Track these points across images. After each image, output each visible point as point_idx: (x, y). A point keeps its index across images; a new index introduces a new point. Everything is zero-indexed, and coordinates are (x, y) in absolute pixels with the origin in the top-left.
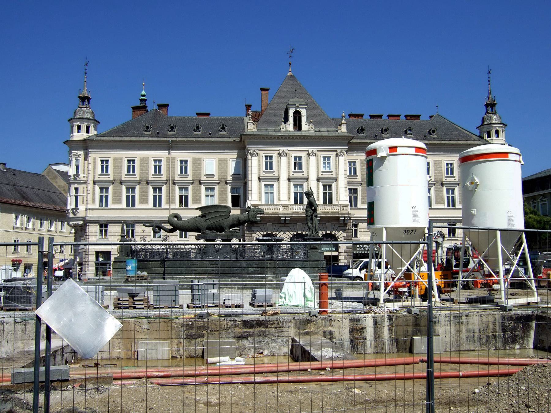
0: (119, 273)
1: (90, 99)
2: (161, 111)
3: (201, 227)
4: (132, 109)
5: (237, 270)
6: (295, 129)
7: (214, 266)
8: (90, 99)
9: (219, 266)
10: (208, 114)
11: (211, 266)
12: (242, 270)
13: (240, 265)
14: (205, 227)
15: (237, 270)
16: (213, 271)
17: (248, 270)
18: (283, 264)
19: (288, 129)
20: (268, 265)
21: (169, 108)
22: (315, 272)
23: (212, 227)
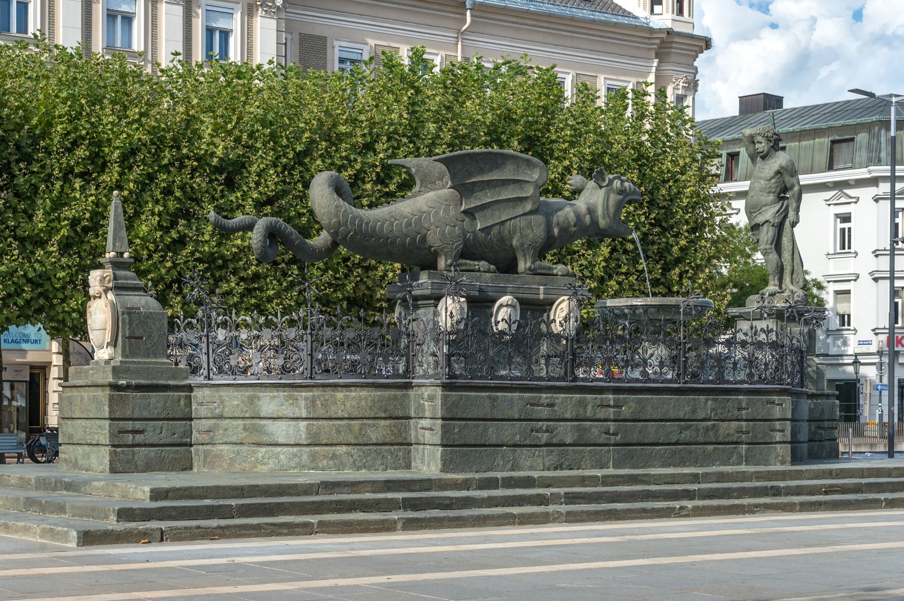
0: (139, 438)
11: (601, 414)
14: (458, 245)
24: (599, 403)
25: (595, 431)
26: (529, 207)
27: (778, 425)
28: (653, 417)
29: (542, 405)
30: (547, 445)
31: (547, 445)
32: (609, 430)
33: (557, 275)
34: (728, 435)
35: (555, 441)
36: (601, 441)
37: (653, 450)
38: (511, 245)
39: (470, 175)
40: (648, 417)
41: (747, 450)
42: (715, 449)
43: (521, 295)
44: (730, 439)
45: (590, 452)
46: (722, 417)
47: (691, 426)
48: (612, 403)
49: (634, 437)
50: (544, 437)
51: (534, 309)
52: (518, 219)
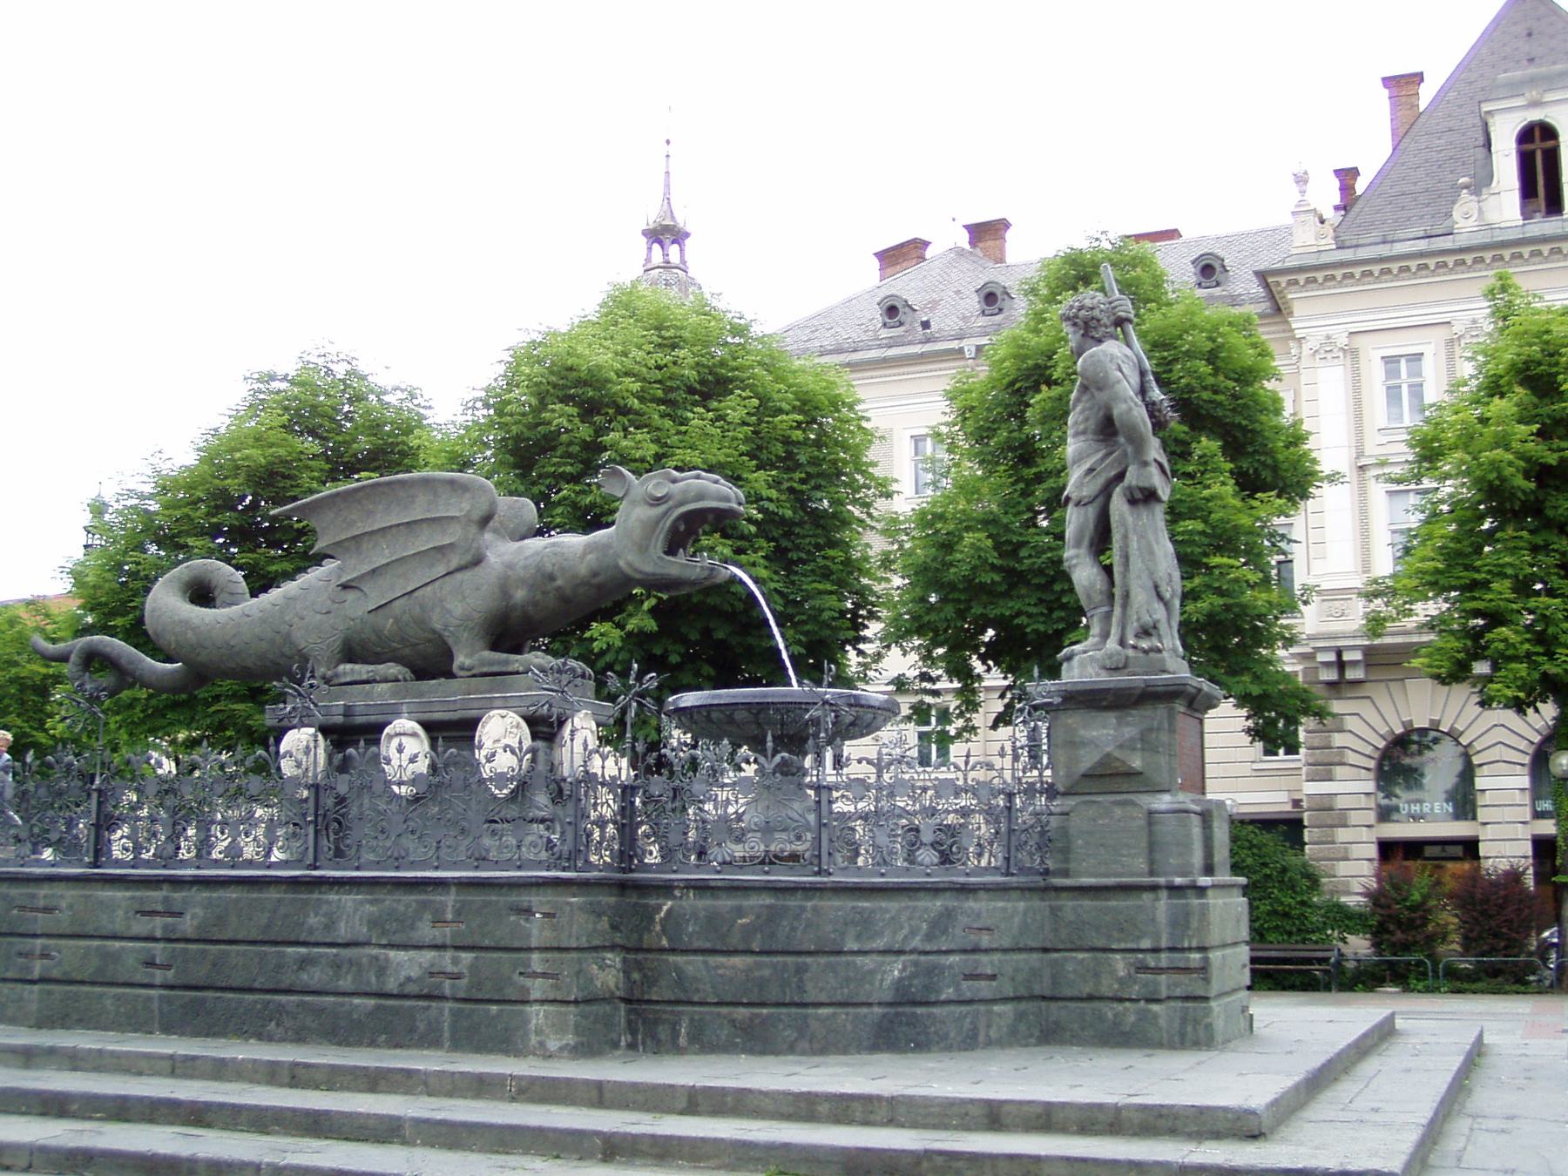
1: (687, 235)
2: (978, 251)
3: (303, 640)
4: (876, 263)
5: (304, 963)
6: (1527, 214)
7: (157, 925)
8: (687, 235)
9: (187, 925)
10: (1172, 234)
11: (141, 926)
12: (337, 965)
13: (330, 926)
15: (304, 963)
16: (150, 964)
17: (382, 969)
18: (713, 921)
19: (1492, 217)
20: (537, 930)
21: (1009, 235)
22: (1107, 987)
23: (378, 633)
24: (137, 907)
25: (130, 961)
26: (455, 562)
27: (536, 961)
28: (240, 937)
29: (37, 910)
30: (43, 980)
31: (43, 980)
32: (154, 957)
33: (518, 673)
34: (409, 979)
35: (55, 973)
36: (138, 978)
37: (240, 1002)
38: (434, 632)
39: (351, 524)
40: (228, 935)
41: (455, 1014)
42: (378, 1007)
43: (427, 717)
44: (412, 988)
45: (117, 998)
46: (397, 939)
47: (321, 955)
48: (160, 908)
49: (200, 974)
50: (38, 967)
51: (453, 733)
52: (437, 584)
